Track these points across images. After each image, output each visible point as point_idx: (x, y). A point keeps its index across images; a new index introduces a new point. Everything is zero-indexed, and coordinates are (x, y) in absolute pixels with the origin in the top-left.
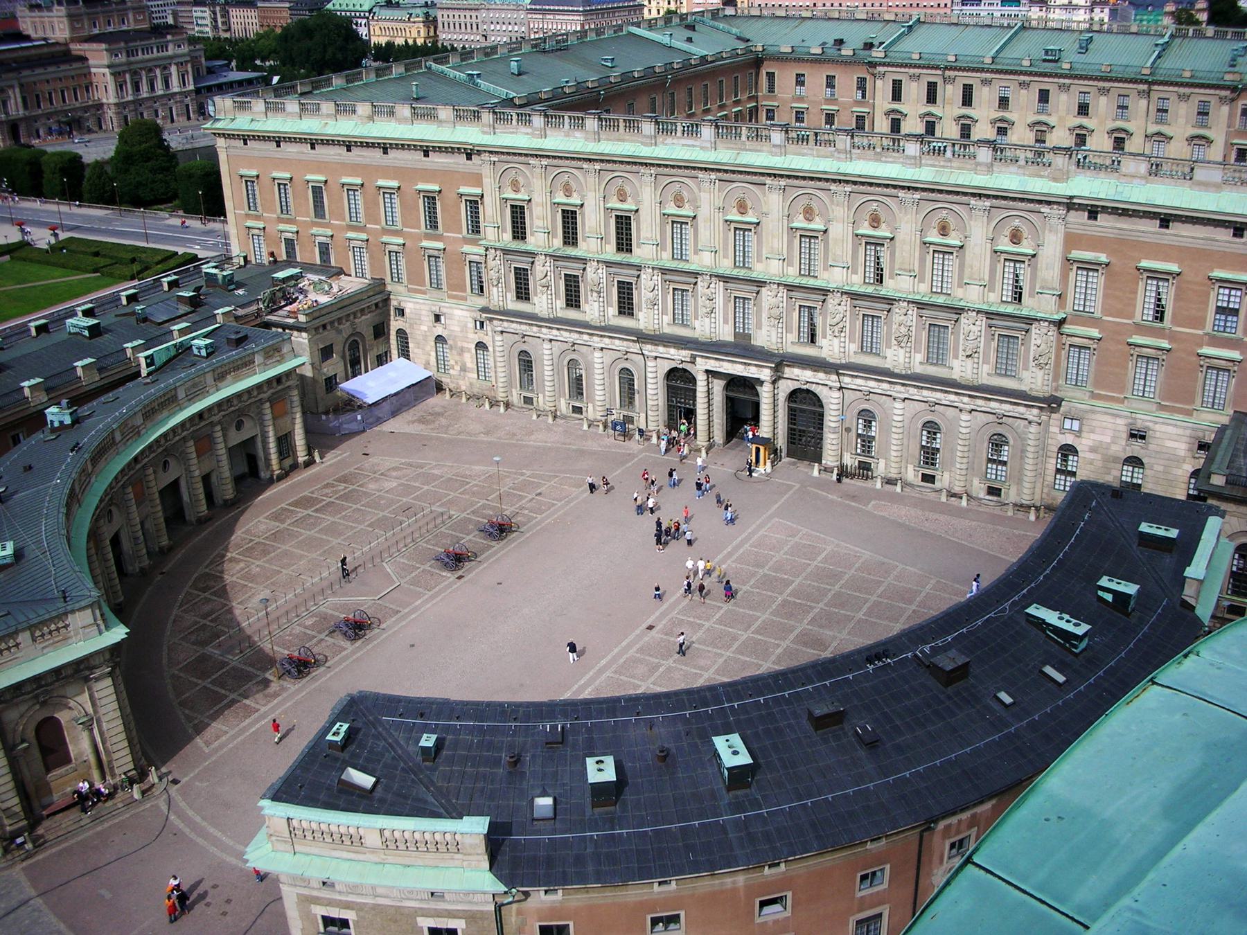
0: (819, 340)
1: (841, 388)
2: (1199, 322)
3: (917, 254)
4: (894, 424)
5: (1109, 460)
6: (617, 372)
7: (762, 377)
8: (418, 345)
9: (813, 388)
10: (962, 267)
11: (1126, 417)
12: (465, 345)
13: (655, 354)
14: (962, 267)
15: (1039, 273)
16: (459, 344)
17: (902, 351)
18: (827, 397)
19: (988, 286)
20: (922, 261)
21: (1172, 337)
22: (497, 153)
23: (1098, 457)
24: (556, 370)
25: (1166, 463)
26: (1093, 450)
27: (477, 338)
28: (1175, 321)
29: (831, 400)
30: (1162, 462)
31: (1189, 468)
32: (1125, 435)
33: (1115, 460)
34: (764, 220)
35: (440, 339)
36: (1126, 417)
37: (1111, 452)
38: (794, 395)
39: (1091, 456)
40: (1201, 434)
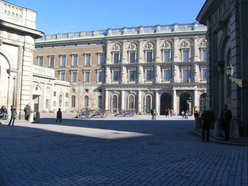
12: (94, 97)
16: (92, 97)
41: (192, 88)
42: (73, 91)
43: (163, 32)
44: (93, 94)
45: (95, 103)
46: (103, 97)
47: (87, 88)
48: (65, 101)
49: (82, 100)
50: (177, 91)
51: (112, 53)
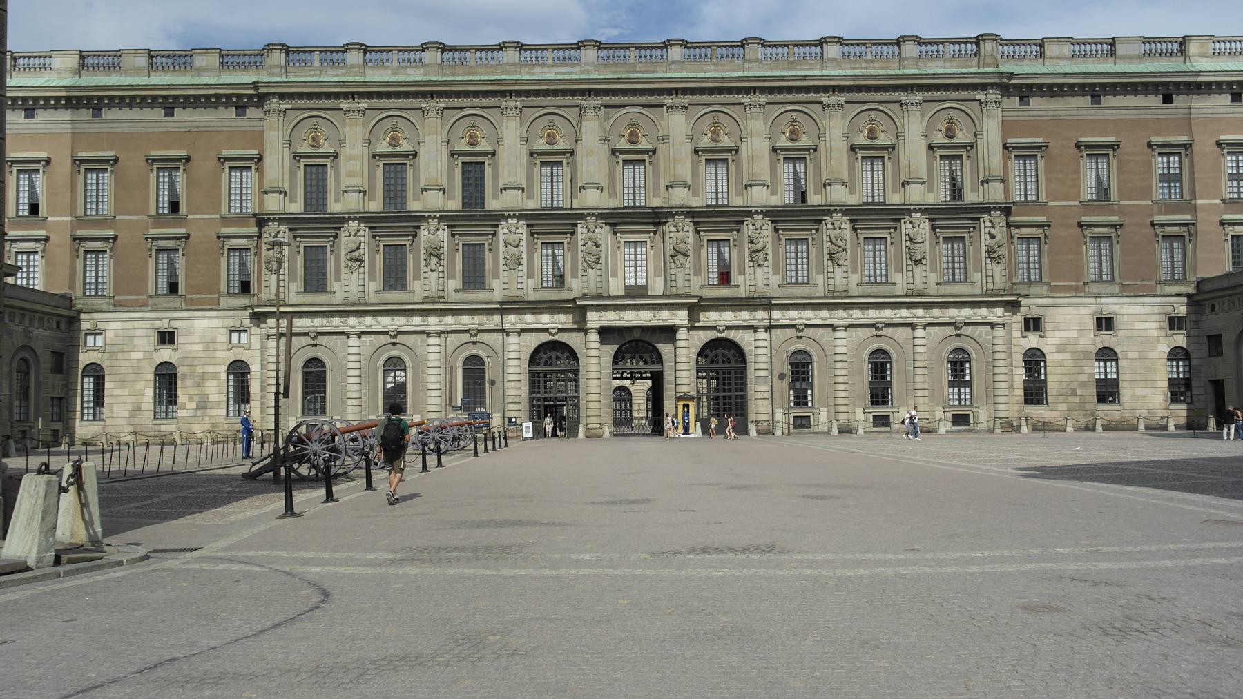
0: (736, 278)
1: (770, 328)
2: (1146, 192)
3: (845, 162)
4: (838, 358)
5: (1080, 356)
7: (677, 323)
8: (122, 383)
9: (731, 335)
10: (896, 170)
11: (1090, 305)
12: (209, 369)
13: (519, 327)
14: (896, 170)
15: (981, 164)
16: (199, 369)
17: (838, 271)
18: (750, 344)
19: (927, 183)
20: (851, 169)
21: (1122, 211)
22: (291, 96)
23: (1067, 356)
24: (366, 375)
25: (1140, 347)
26: (1060, 349)
28: (1122, 196)
29: (756, 346)
30: (1135, 348)
31: (1165, 348)
32: (1092, 325)
33: (1086, 355)
34: (661, 148)
36: (1090, 305)
37: (1080, 348)
38: (706, 351)
39: (1061, 356)
40: (1169, 309)
41: (665, 318)
44: (201, 355)
45: (213, 397)
46: (255, 368)
47: (164, 325)
49: (141, 384)
50: (606, 333)
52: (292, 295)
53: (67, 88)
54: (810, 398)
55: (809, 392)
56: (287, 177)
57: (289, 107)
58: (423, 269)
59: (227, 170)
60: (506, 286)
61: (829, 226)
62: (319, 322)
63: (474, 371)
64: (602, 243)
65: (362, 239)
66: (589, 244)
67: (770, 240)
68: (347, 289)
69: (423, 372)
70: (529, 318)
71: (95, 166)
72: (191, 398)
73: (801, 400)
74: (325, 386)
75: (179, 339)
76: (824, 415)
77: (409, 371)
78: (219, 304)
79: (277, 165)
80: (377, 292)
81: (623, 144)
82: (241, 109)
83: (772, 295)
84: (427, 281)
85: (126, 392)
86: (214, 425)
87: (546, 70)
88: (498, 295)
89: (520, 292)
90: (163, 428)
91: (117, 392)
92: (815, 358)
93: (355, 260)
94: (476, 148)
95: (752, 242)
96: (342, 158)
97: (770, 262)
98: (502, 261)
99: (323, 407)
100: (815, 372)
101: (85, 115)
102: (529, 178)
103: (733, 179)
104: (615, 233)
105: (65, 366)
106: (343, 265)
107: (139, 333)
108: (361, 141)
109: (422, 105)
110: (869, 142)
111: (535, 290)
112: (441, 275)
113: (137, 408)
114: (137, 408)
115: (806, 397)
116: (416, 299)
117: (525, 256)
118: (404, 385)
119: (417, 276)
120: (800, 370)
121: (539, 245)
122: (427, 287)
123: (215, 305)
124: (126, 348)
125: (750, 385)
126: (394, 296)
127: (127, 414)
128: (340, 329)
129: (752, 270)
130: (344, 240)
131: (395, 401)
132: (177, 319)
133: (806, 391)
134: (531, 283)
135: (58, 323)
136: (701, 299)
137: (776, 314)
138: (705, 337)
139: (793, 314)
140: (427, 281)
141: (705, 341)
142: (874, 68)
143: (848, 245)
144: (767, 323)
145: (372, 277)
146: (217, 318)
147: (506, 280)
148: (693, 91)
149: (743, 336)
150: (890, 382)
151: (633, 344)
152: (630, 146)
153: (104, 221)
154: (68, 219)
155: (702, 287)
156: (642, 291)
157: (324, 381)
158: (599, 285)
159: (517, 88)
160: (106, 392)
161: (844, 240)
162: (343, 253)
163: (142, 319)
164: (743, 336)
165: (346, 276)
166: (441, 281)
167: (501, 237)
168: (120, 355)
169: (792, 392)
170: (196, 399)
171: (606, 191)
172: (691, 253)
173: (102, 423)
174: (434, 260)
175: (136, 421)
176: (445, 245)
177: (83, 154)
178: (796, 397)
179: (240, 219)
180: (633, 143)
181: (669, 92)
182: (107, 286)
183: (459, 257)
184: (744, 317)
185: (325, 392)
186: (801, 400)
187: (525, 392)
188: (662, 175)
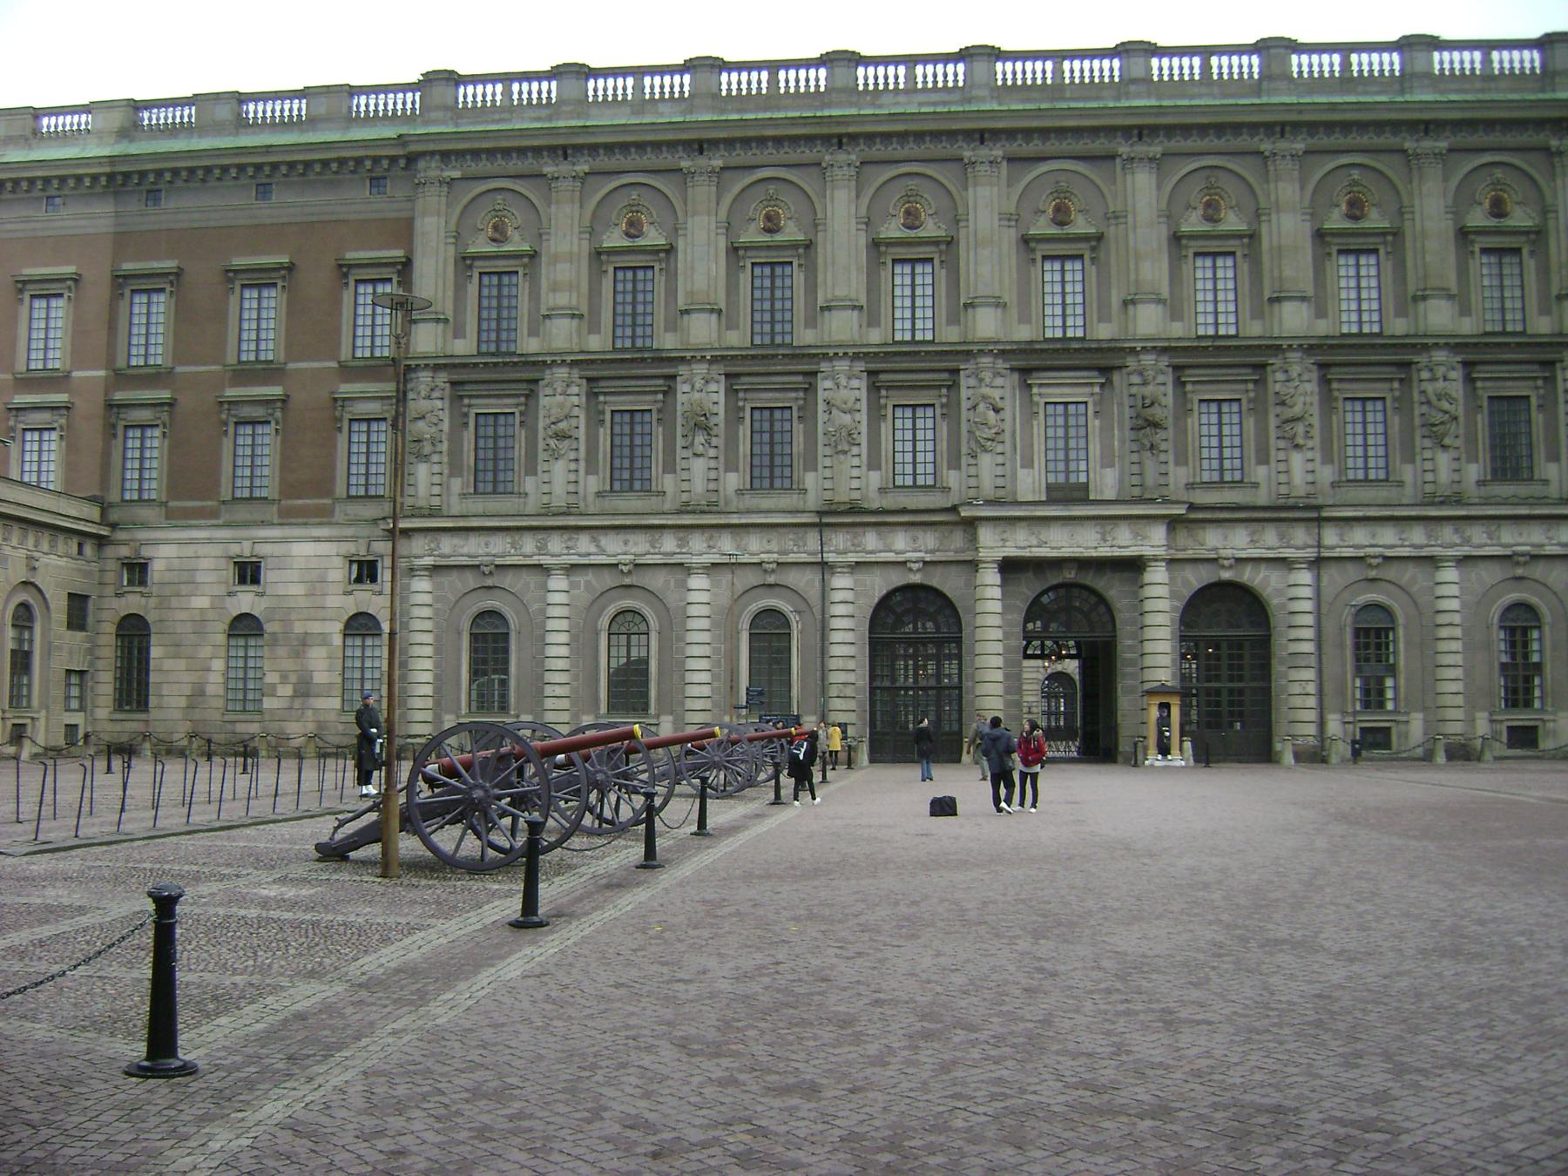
1: (1317, 563)
3: (1452, 259)
4: (1441, 619)
6: (745, 624)
7: (1147, 551)
8: (175, 648)
9: (1247, 576)
10: (1544, 272)
12: (315, 627)
13: (852, 558)
14: (1544, 272)
16: (299, 628)
17: (1443, 460)
18: (1279, 592)
20: (1463, 271)
24: (582, 643)
27: (350, 605)
29: (1295, 599)
35: (245, 626)
41: (1123, 543)
42: (131, 583)
43: (880, 106)
44: (303, 602)
45: (320, 678)
47: (245, 550)
48: (60, 663)
49: (206, 652)
50: (1010, 568)
51: (465, 262)
52: (454, 500)
53: (112, 159)
54: (1389, 694)
55: (1389, 682)
56: (450, 293)
57: (457, 174)
58: (680, 453)
59: (352, 284)
60: (828, 484)
61: (1425, 375)
62: (497, 547)
63: (770, 636)
64: (1007, 404)
65: (575, 400)
66: (981, 407)
67: (1316, 399)
68: (546, 488)
69: (681, 639)
70: (871, 540)
71: (148, 284)
72: (284, 679)
73: (1373, 697)
74: (506, 661)
75: (267, 576)
76: (1416, 727)
77: (654, 636)
78: (331, 513)
79: (432, 277)
80: (599, 494)
81: (1043, 226)
82: (376, 182)
83: (1320, 501)
84: (685, 475)
85: (182, 664)
86: (321, 725)
87: (901, 99)
88: (812, 501)
89: (856, 495)
90: (240, 728)
91: (168, 664)
92: (1401, 620)
93: (561, 436)
94: (778, 237)
95: (1283, 403)
96: (544, 259)
97: (1316, 442)
98: (821, 439)
99: (504, 697)
100: (1401, 646)
101: (133, 206)
102: (872, 288)
103: (1245, 287)
104: (1030, 386)
105: (90, 619)
106: (541, 445)
107: (205, 563)
108: (576, 230)
109: (684, 164)
110: (1493, 222)
111: (882, 490)
112: (713, 464)
113: (199, 692)
114: (199, 692)
115: (1381, 692)
116: (667, 507)
117: (864, 428)
118: (646, 661)
119: (670, 467)
120: (1373, 639)
121: (890, 409)
122: (685, 486)
123: (323, 515)
124: (184, 589)
125: (1277, 668)
126: (632, 503)
127: (183, 702)
128: (534, 560)
129: (1281, 455)
130: (544, 401)
131: (630, 686)
132: (266, 541)
133: (1380, 681)
134: (875, 479)
135: (80, 545)
136: (1192, 507)
137: (1330, 536)
138: (1196, 578)
139: (1360, 535)
140: (685, 475)
141: (1196, 585)
142: (1497, 90)
143: (1460, 412)
144: (1311, 553)
145: (591, 469)
146: (328, 540)
147: (828, 473)
148: (1170, 130)
149: (1266, 578)
150: (1538, 667)
151: (1062, 592)
152: (1054, 231)
153: (155, 377)
154: (102, 373)
155: (1190, 486)
156: (1076, 494)
157: (506, 651)
158: (1000, 482)
159: (851, 130)
160: (152, 663)
161: (1451, 400)
162: (541, 425)
163: (210, 541)
164: (1266, 578)
165: (546, 467)
166: (713, 475)
167: (821, 395)
168: (174, 602)
169: (1358, 683)
170: (293, 678)
171: (1014, 312)
172: (1170, 423)
173: (143, 716)
174: (700, 438)
175: (197, 715)
176: (721, 409)
177: (128, 266)
178: (1366, 692)
179: (370, 369)
180: (1062, 224)
181: (1126, 131)
182: (155, 487)
183: (744, 431)
184: (1269, 541)
185: (506, 671)
186: (1373, 697)
187: (861, 678)
188: (1114, 281)
